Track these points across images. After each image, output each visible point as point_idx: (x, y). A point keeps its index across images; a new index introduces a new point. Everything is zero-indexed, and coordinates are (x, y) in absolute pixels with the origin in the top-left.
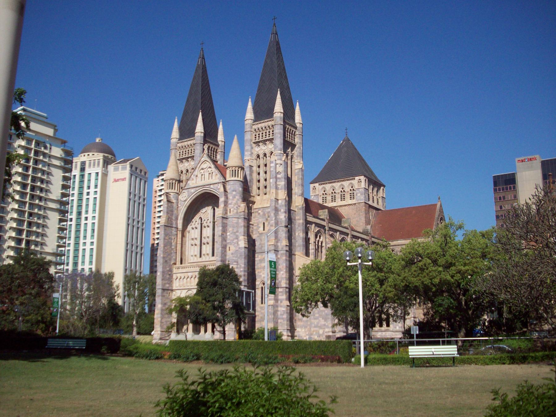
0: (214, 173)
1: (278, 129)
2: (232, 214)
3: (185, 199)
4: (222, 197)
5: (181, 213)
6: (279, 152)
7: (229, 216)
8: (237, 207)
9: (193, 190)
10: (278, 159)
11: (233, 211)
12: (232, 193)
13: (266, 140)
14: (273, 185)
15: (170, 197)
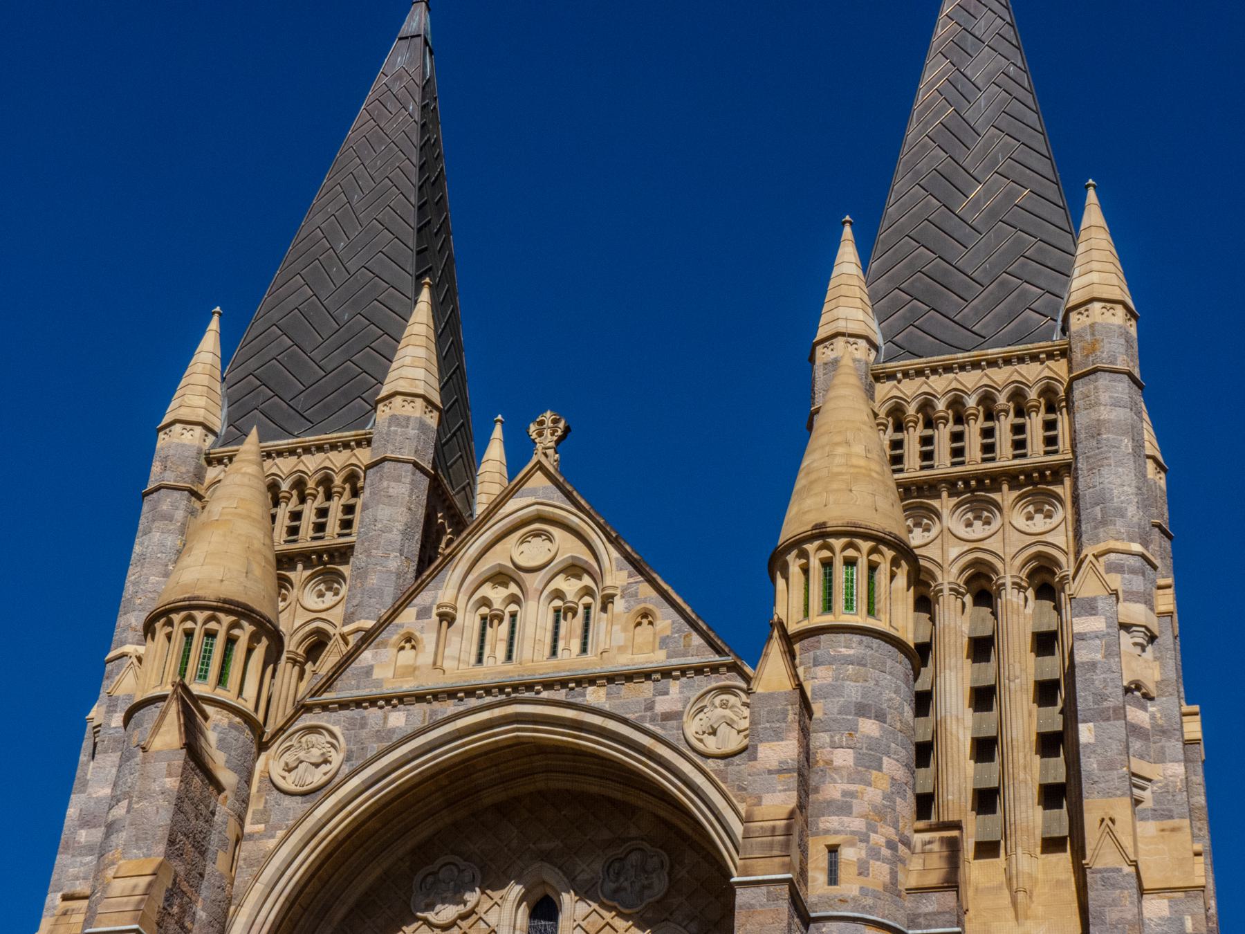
0: (619, 605)
1: (1116, 404)
2: (850, 886)
3: (317, 777)
4: (778, 736)
5: (259, 887)
6: (1137, 547)
7: (828, 901)
8: (891, 845)
9: (398, 719)
10: (1132, 597)
11: (863, 870)
12: (853, 730)
13: (995, 480)
14: (1110, 766)
15: (203, 733)
